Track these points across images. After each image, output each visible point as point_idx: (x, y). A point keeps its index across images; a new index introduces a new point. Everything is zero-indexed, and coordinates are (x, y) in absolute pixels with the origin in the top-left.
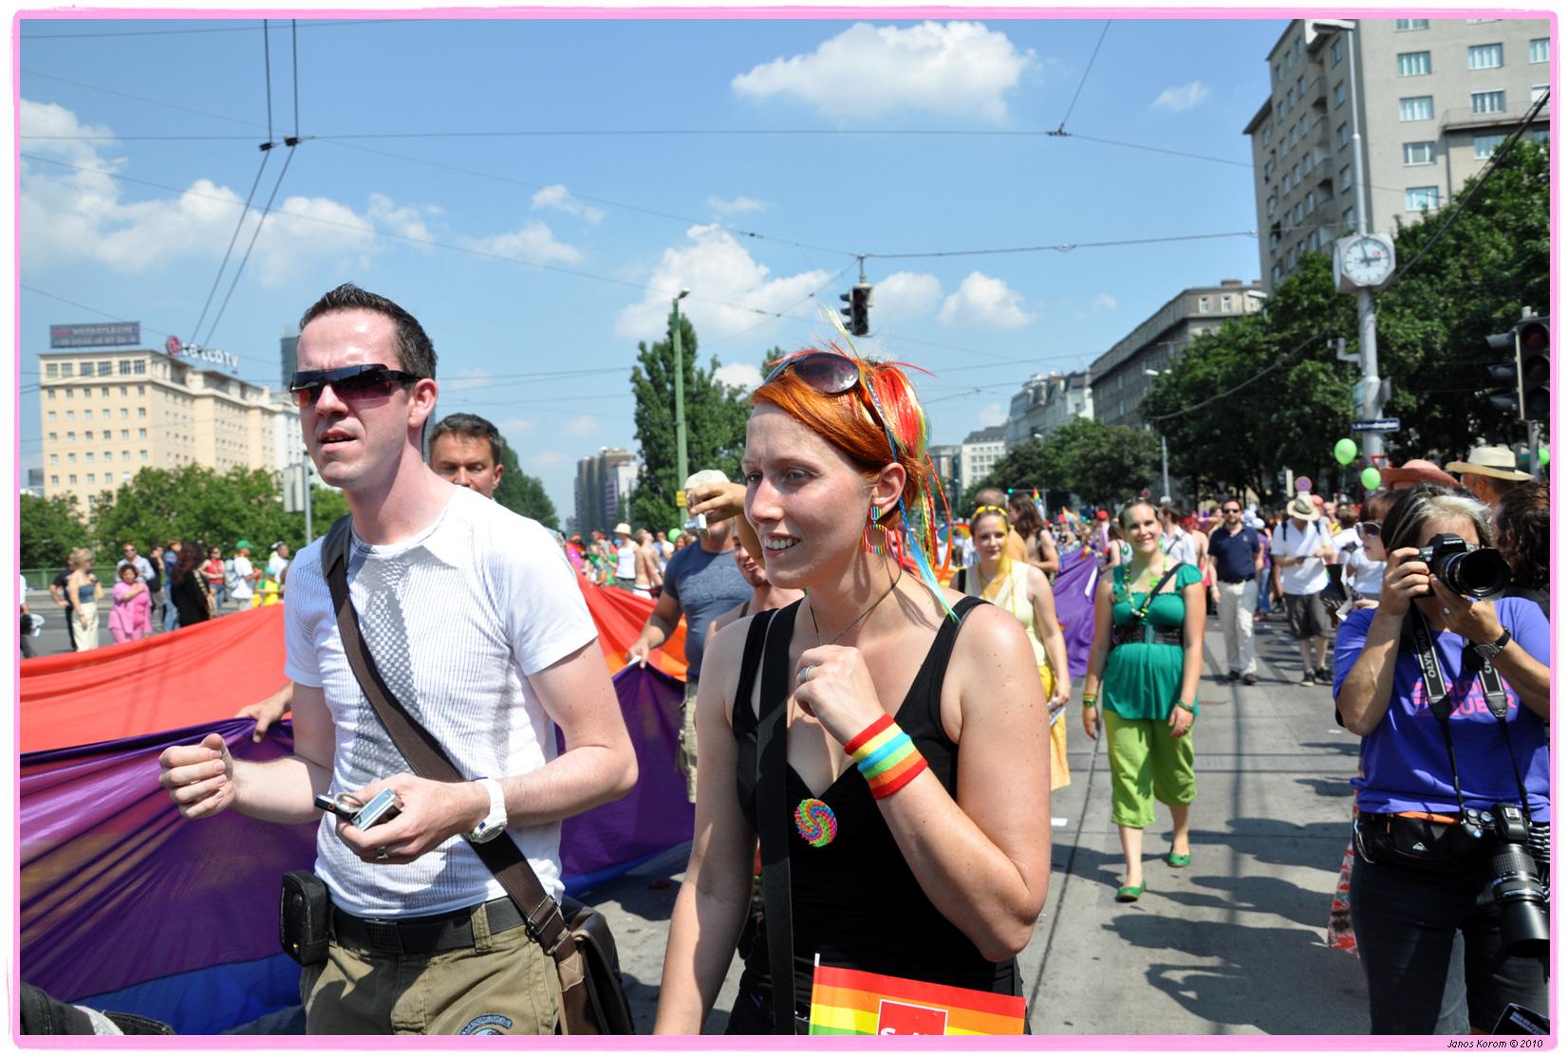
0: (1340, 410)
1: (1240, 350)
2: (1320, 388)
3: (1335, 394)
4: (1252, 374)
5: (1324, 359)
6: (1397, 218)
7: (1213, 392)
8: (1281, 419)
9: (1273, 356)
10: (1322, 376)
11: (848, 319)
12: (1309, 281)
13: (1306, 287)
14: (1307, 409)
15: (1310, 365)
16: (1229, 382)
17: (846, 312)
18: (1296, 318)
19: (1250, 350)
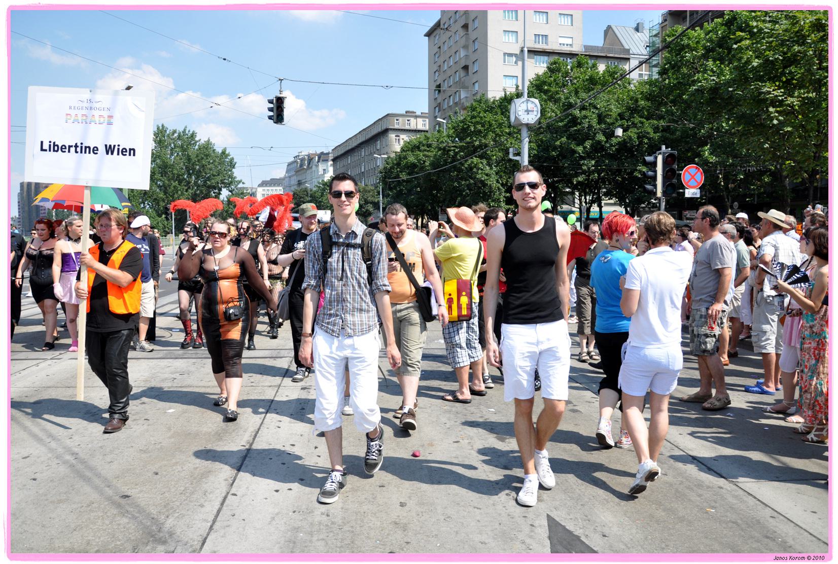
0: (489, 183)
1: (440, 149)
2: (480, 171)
3: (487, 175)
4: (446, 163)
5: (481, 157)
6: (505, 90)
7: (422, 168)
8: (460, 185)
9: (456, 154)
10: (481, 166)
11: (271, 114)
12: (473, 117)
13: (474, 120)
14: (472, 181)
15: (475, 160)
16: (434, 165)
17: (271, 110)
18: (468, 135)
19: (444, 149)
